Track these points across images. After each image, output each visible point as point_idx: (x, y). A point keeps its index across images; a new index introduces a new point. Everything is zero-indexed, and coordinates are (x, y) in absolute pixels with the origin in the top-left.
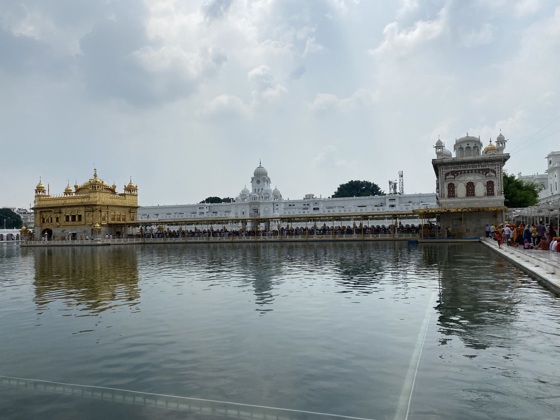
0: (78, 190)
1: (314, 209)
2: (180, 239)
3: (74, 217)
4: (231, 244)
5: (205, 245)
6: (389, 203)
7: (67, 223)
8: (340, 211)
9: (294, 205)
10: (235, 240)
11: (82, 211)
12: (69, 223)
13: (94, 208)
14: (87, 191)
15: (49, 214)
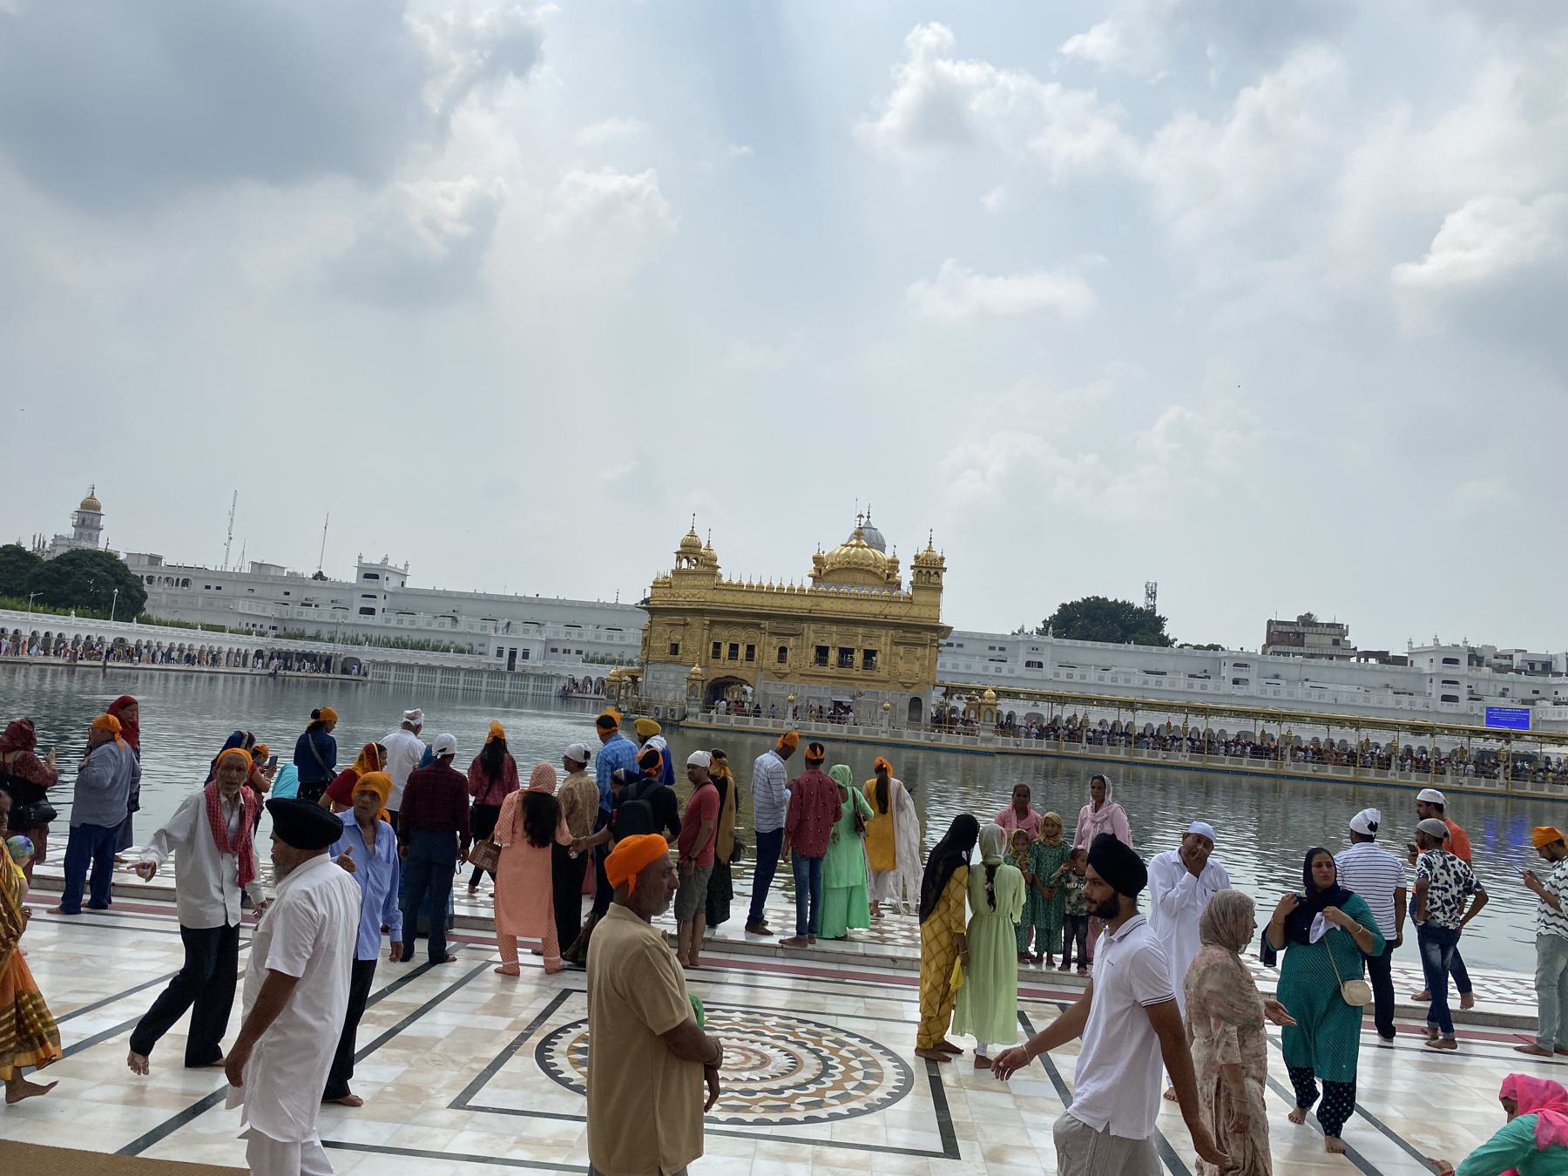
0: (824, 570)
1: (1028, 664)
2: (1183, 757)
3: (845, 653)
4: (1351, 788)
5: (1266, 782)
6: (1228, 672)
7: (818, 669)
8: (1101, 679)
9: (960, 646)
10: (1365, 778)
11: (883, 642)
12: (827, 670)
13: (929, 636)
14: (860, 577)
15: (742, 637)
